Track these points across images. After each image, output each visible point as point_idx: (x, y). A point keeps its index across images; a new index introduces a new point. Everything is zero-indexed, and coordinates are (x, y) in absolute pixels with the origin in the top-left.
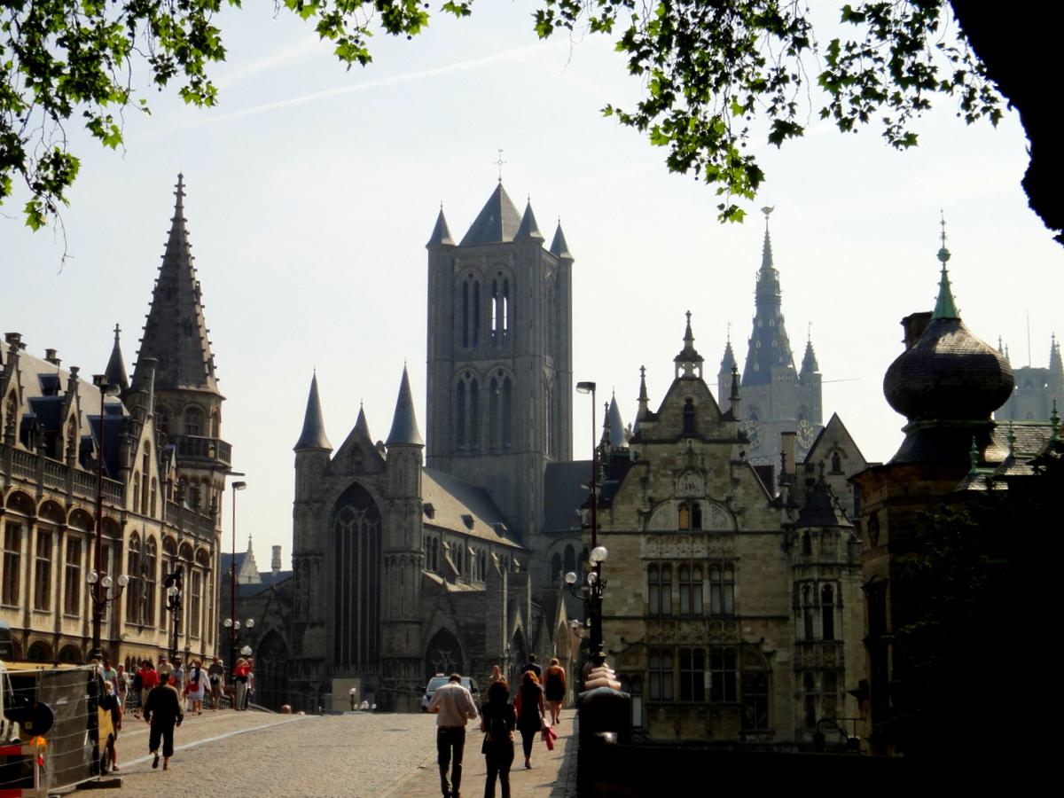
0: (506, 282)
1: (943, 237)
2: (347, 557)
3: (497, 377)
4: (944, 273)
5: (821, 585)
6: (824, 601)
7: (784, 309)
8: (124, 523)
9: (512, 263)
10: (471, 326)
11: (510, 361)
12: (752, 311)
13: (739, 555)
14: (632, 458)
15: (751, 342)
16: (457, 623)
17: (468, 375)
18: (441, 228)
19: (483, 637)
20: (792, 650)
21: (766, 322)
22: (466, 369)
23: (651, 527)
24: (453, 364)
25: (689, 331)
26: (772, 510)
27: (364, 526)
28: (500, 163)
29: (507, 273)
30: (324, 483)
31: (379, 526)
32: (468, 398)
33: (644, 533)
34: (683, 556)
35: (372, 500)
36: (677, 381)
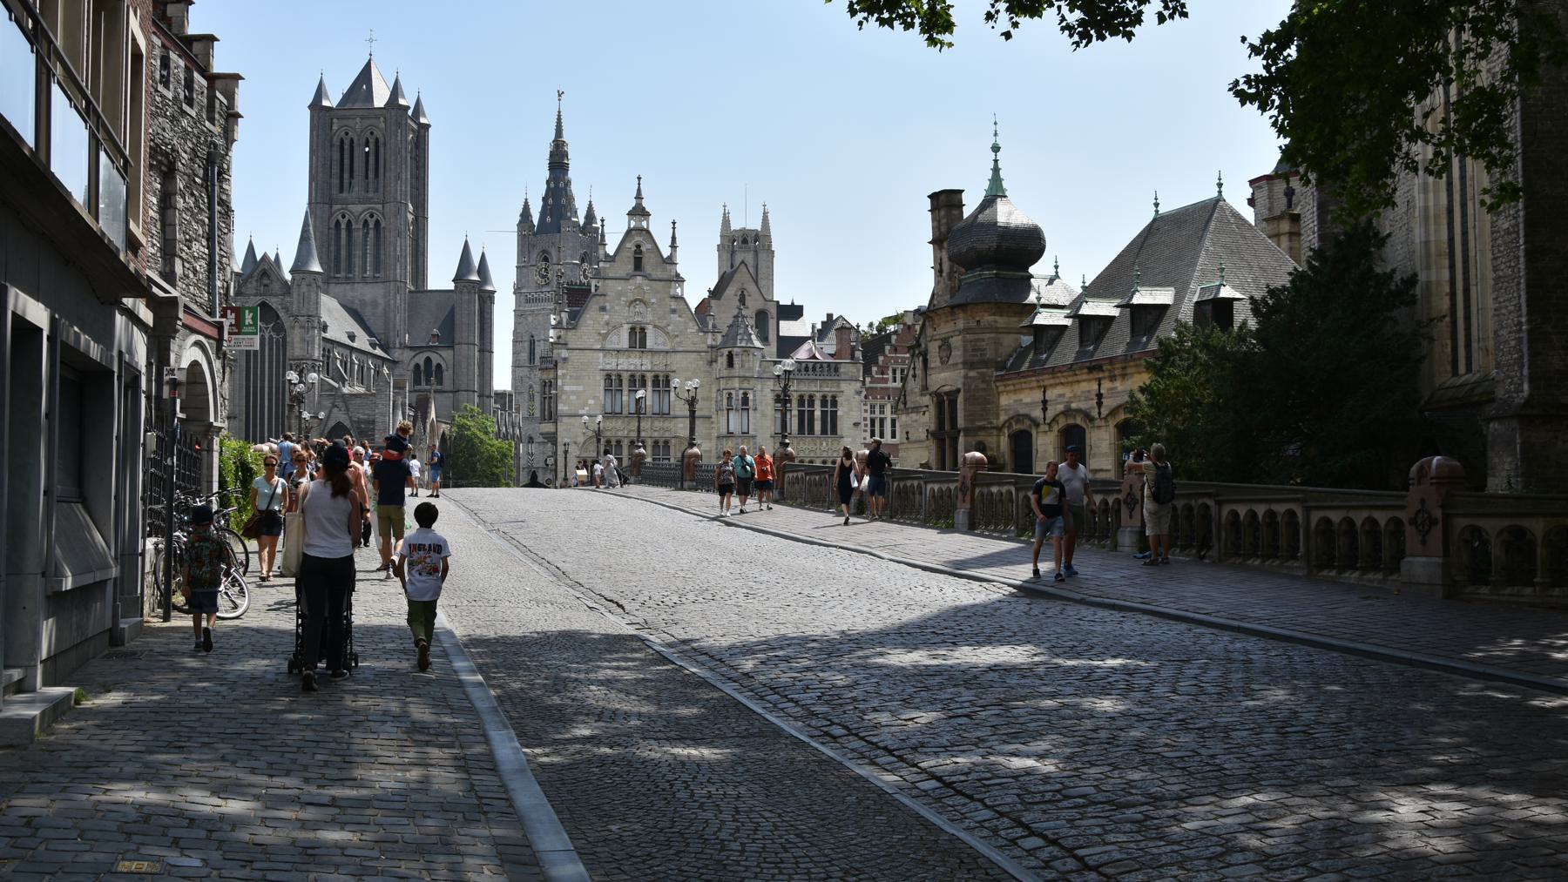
0: (377, 141)
1: (996, 135)
3: (369, 219)
4: (996, 161)
5: (741, 392)
6: (743, 405)
7: (572, 174)
9: (383, 125)
10: (346, 176)
11: (379, 207)
12: (546, 174)
14: (593, 290)
15: (544, 199)
16: (350, 418)
17: (344, 217)
18: (320, 93)
19: (374, 429)
20: (714, 441)
21: (557, 185)
23: (608, 346)
26: (701, 334)
28: (371, 40)
29: (378, 134)
31: (284, 339)
32: (344, 234)
33: (602, 350)
34: (632, 368)
35: (278, 317)
36: (629, 231)
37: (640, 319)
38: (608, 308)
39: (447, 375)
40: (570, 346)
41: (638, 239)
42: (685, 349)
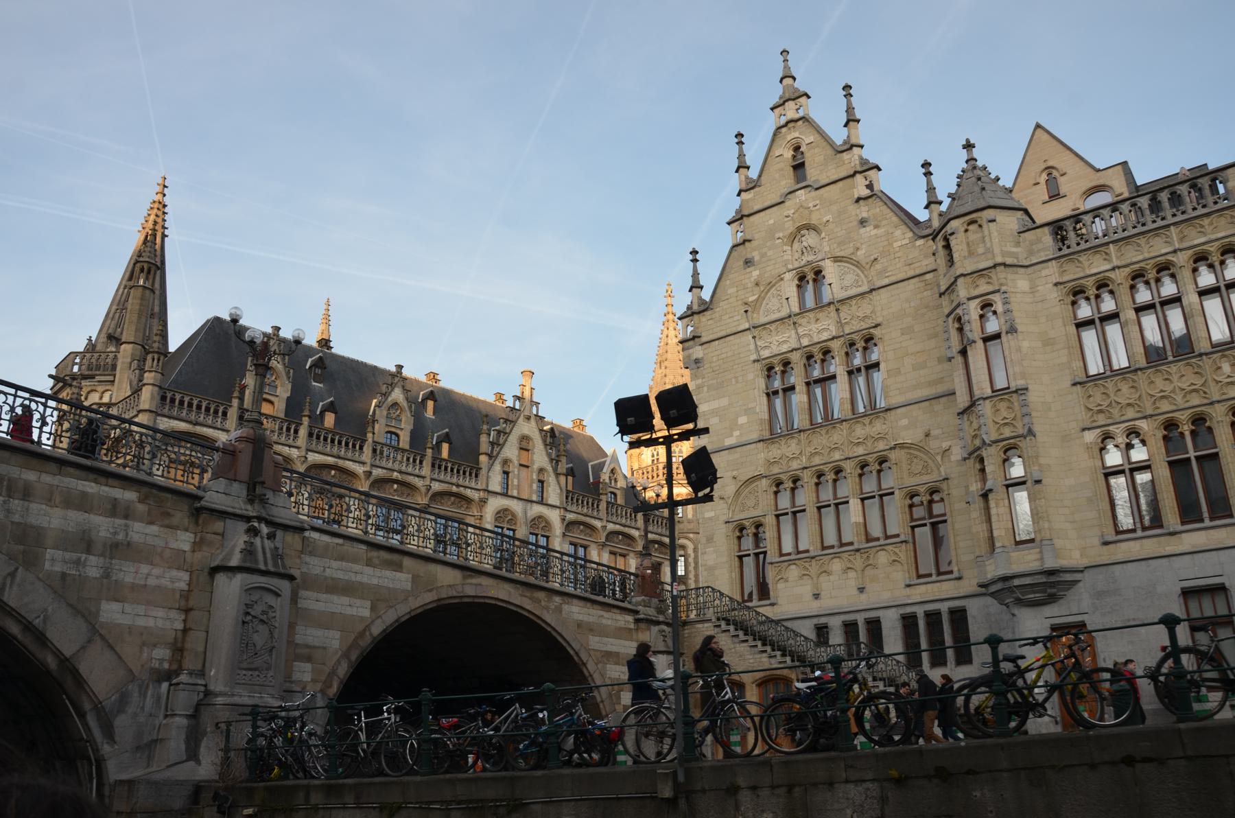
8: (483, 502)
13: (879, 320)
25: (850, 109)
37: (811, 258)
38: (757, 258)
40: (704, 339)
41: (791, 135)
42: (893, 279)
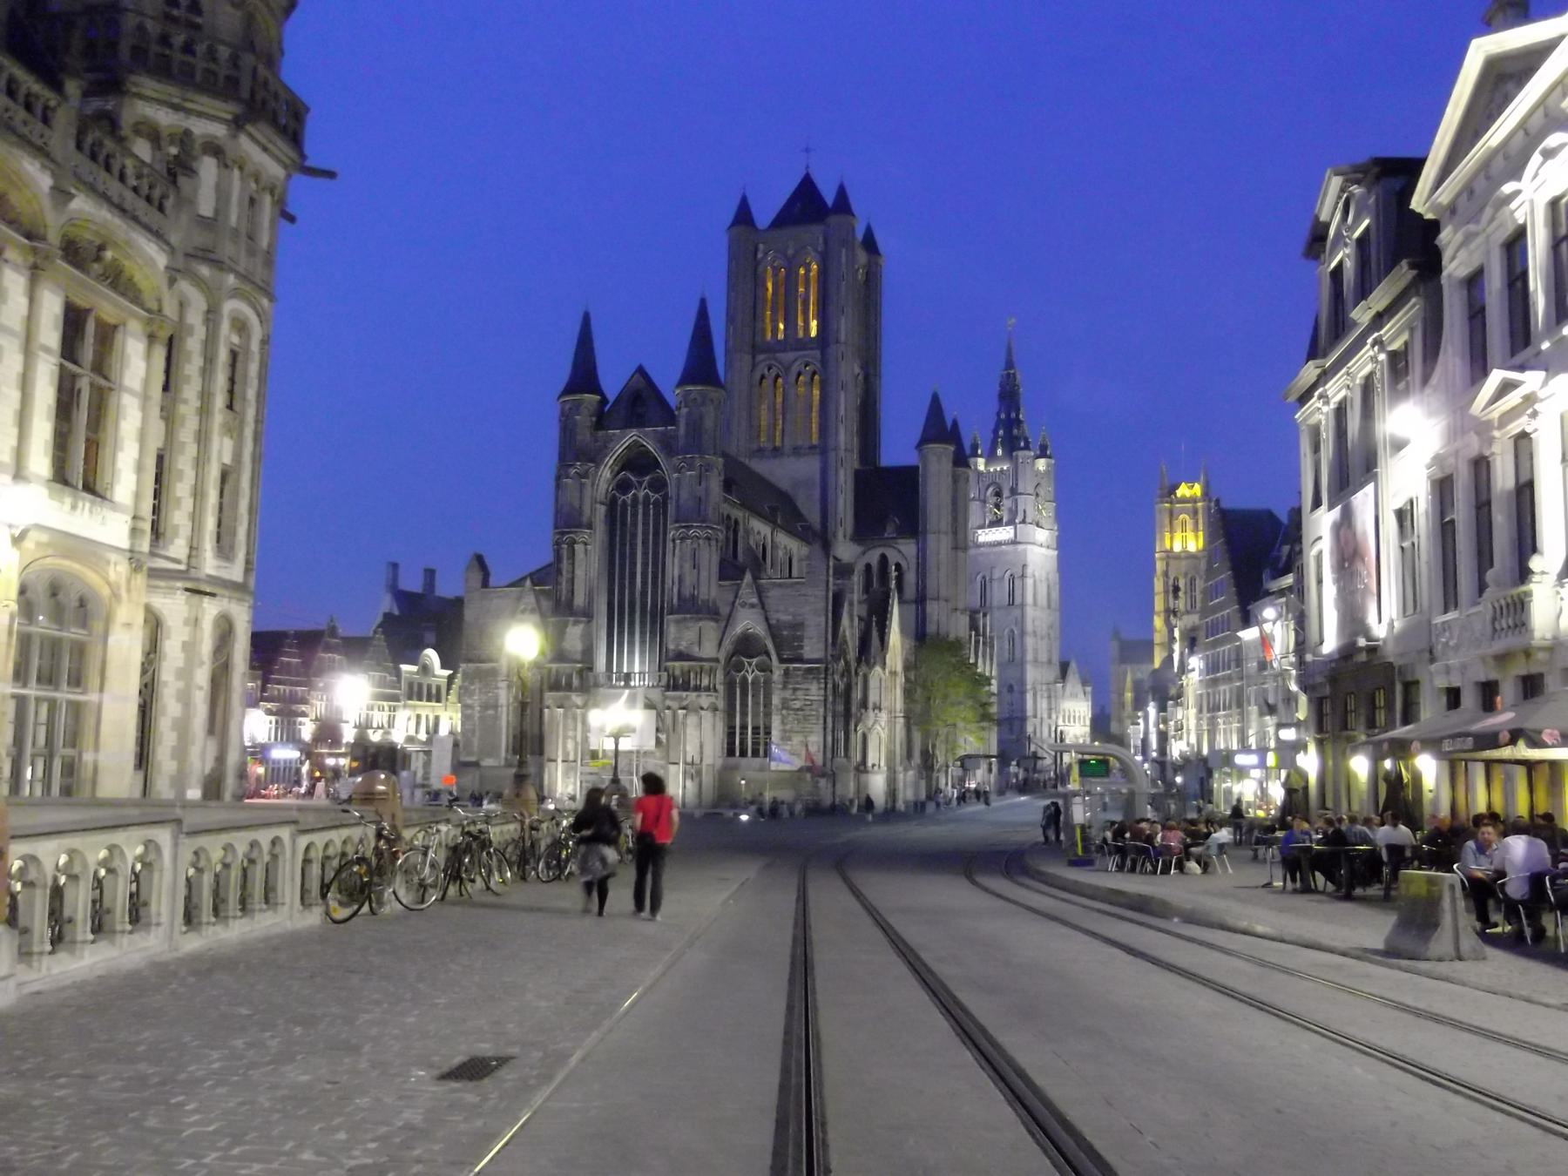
2: (623, 545)
19: (801, 639)
21: (1008, 415)
22: (768, 362)
24: (754, 357)
27: (647, 497)
28: (807, 150)
30: (596, 441)
39: (910, 578)
